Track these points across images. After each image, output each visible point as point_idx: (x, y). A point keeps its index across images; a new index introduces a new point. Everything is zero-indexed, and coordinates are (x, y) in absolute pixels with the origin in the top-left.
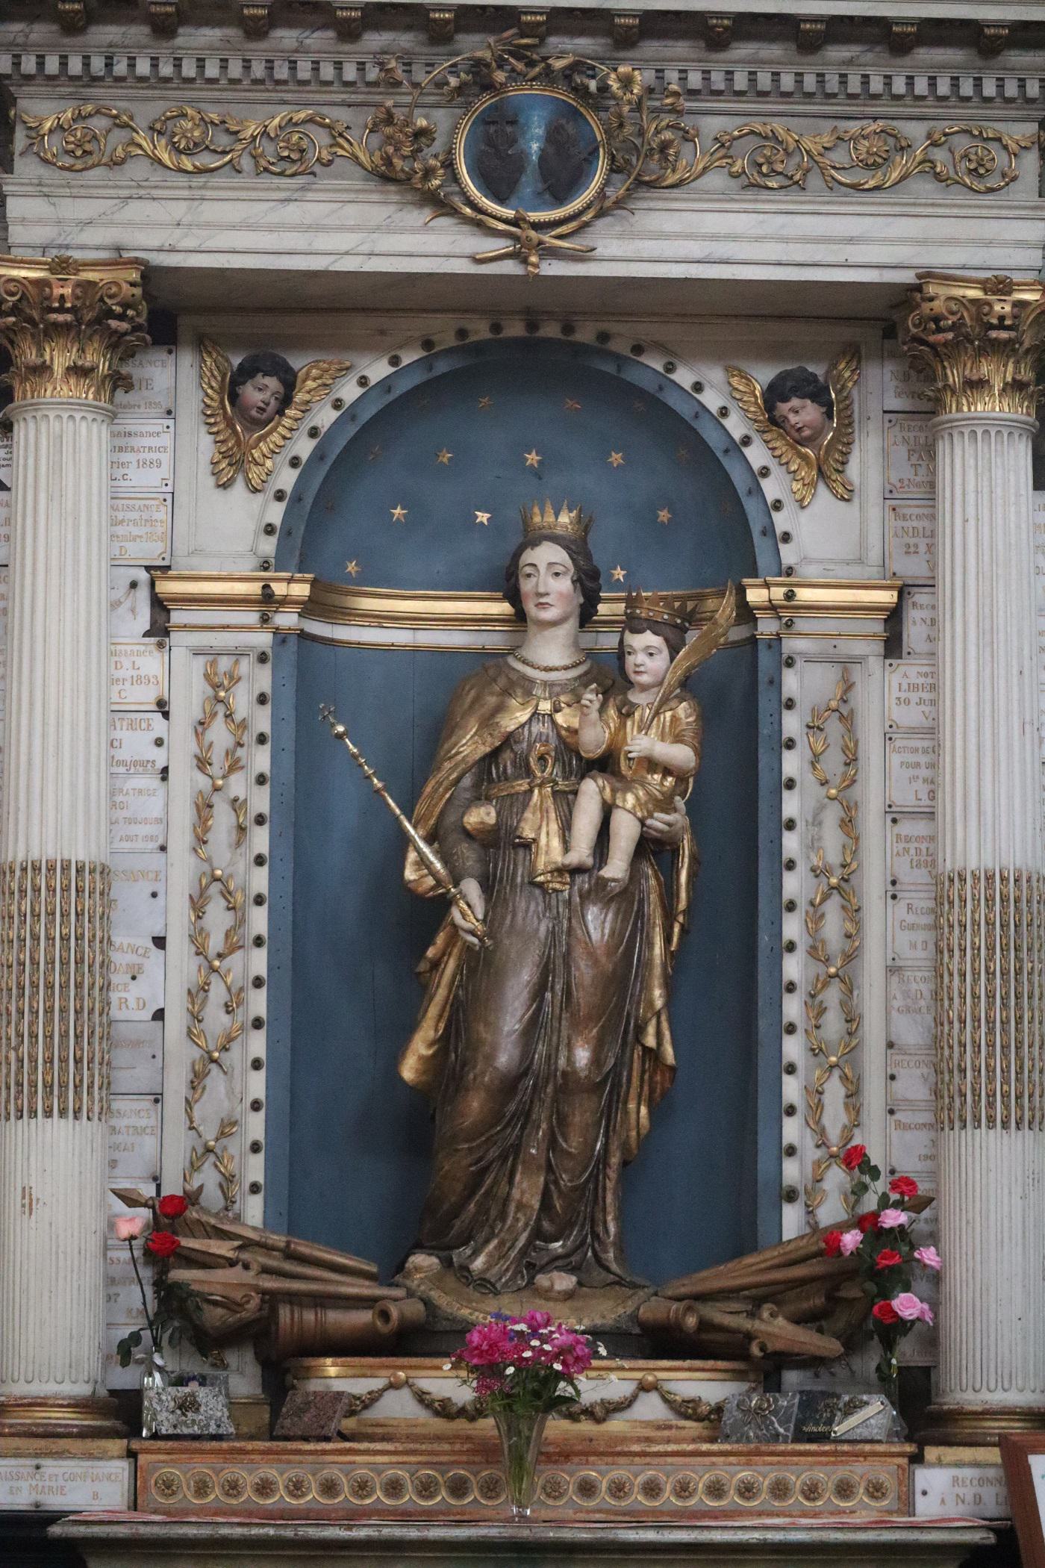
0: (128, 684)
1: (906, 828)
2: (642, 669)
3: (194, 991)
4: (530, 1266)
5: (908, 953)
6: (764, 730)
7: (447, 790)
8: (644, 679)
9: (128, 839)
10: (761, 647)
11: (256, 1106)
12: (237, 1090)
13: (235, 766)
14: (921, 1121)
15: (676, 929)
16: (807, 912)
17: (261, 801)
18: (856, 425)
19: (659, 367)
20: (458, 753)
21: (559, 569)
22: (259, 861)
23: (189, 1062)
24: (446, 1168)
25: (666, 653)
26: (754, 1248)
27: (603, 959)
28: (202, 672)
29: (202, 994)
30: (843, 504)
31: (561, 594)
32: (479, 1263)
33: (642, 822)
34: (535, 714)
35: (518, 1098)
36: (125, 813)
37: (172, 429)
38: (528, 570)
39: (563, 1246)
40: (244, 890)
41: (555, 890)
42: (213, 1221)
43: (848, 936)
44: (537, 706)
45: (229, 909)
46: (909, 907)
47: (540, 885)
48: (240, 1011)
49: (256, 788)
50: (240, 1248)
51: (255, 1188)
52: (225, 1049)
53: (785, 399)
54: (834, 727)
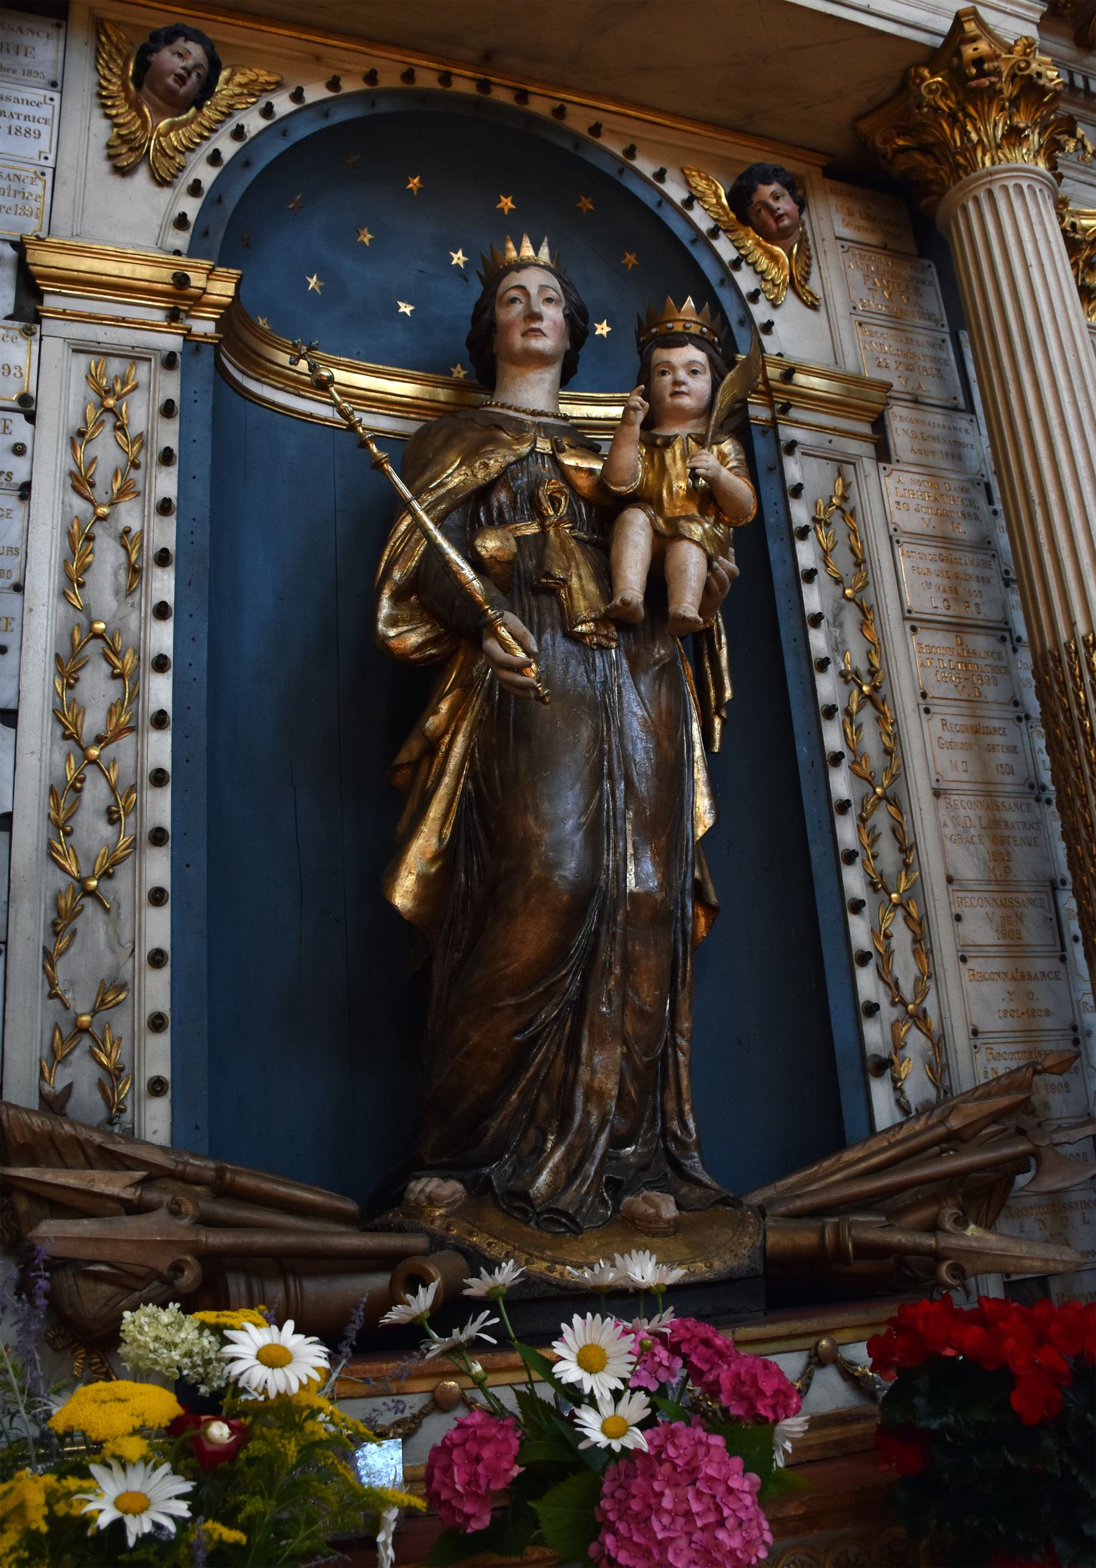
2: (683, 389)
3: (59, 790)
5: (952, 775)
8: (686, 402)
10: (756, 433)
11: (157, 959)
12: (127, 935)
14: (994, 970)
15: (717, 723)
16: (844, 722)
19: (618, 150)
20: (442, 485)
21: (552, 294)
22: (161, 611)
23: (50, 894)
24: (475, 1038)
25: (708, 377)
26: (841, 1144)
28: (83, 372)
29: (71, 795)
30: (809, 312)
31: (555, 323)
33: (710, 560)
34: (533, 451)
37: (57, 103)
38: (514, 293)
40: (137, 652)
41: (600, 646)
42: (98, 1139)
44: (535, 442)
45: (114, 677)
48: (128, 823)
49: (156, 520)
51: (157, 1087)
52: (107, 875)
53: (768, 183)
54: (839, 525)
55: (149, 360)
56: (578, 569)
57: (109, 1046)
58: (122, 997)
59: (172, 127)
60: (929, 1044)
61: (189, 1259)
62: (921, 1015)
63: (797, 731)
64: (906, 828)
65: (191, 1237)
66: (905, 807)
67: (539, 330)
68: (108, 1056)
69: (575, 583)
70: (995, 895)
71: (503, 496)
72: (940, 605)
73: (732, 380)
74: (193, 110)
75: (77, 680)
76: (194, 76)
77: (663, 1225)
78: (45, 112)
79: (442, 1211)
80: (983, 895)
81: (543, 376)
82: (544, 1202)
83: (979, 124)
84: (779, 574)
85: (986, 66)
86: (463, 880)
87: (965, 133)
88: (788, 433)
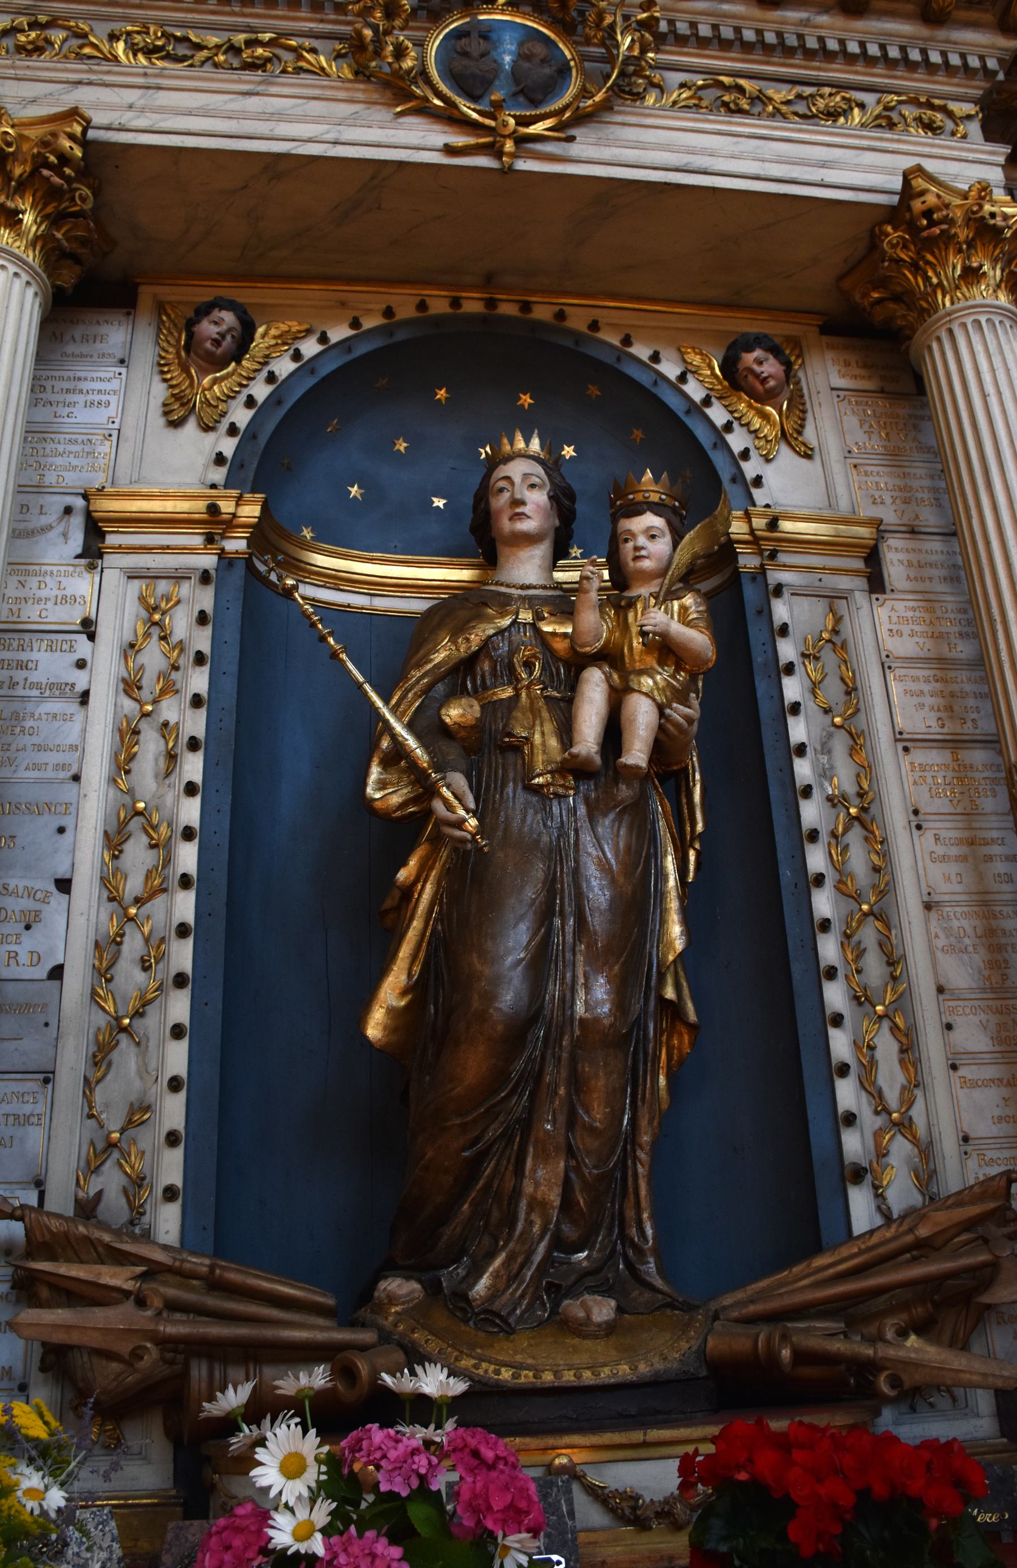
0: (50, 605)
1: (919, 756)
2: (643, 553)
3: (102, 943)
4: (554, 1289)
6: (758, 658)
7: (417, 696)
8: (647, 564)
9: (37, 767)
12: (153, 1065)
13: (169, 689)
15: (692, 856)
16: (829, 844)
17: (196, 724)
18: (806, 397)
19: (616, 341)
21: (537, 480)
22: (191, 789)
24: (430, 1154)
25: (668, 538)
26: (818, 1249)
27: (622, 880)
28: (136, 594)
29: (113, 946)
30: (804, 462)
31: (538, 506)
32: (482, 1286)
33: (661, 708)
35: (526, 1054)
36: (35, 740)
37: (124, 376)
38: (502, 484)
39: (587, 1257)
41: (557, 795)
42: (107, 1238)
43: (877, 870)
44: (517, 614)
45: (152, 847)
46: (937, 838)
47: (537, 790)
49: (189, 712)
50: (143, 1277)
51: (170, 1194)
52: (138, 1014)
53: (750, 350)
54: (828, 656)
55: (190, 578)
56: (542, 726)
57: (133, 1158)
58: (146, 1117)
59: (215, 381)
60: (916, 1150)
61: (149, 1345)
62: (906, 1123)
63: (780, 855)
64: (894, 942)
65: (152, 1327)
66: (894, 921)
67: (523, 514)
68: (132, 1167)
69: (537, 738)
70: (990, 1003)
71: (486, 666)
72: (933, 723)
73: (692, 539)
74: (233, 364)
75: (121, 852)
76: (229, 338)
77: (592, 1328)
78: (115, 384)
79: (398, 1309)
80: (976, 1003)
81: (533, 553)
82: (483, 1304)
83: (938, 269)
84: (766, 709)
85: (935, 216)
86: (432, 1011)
87: (927, 279)
88: (775, 576)
